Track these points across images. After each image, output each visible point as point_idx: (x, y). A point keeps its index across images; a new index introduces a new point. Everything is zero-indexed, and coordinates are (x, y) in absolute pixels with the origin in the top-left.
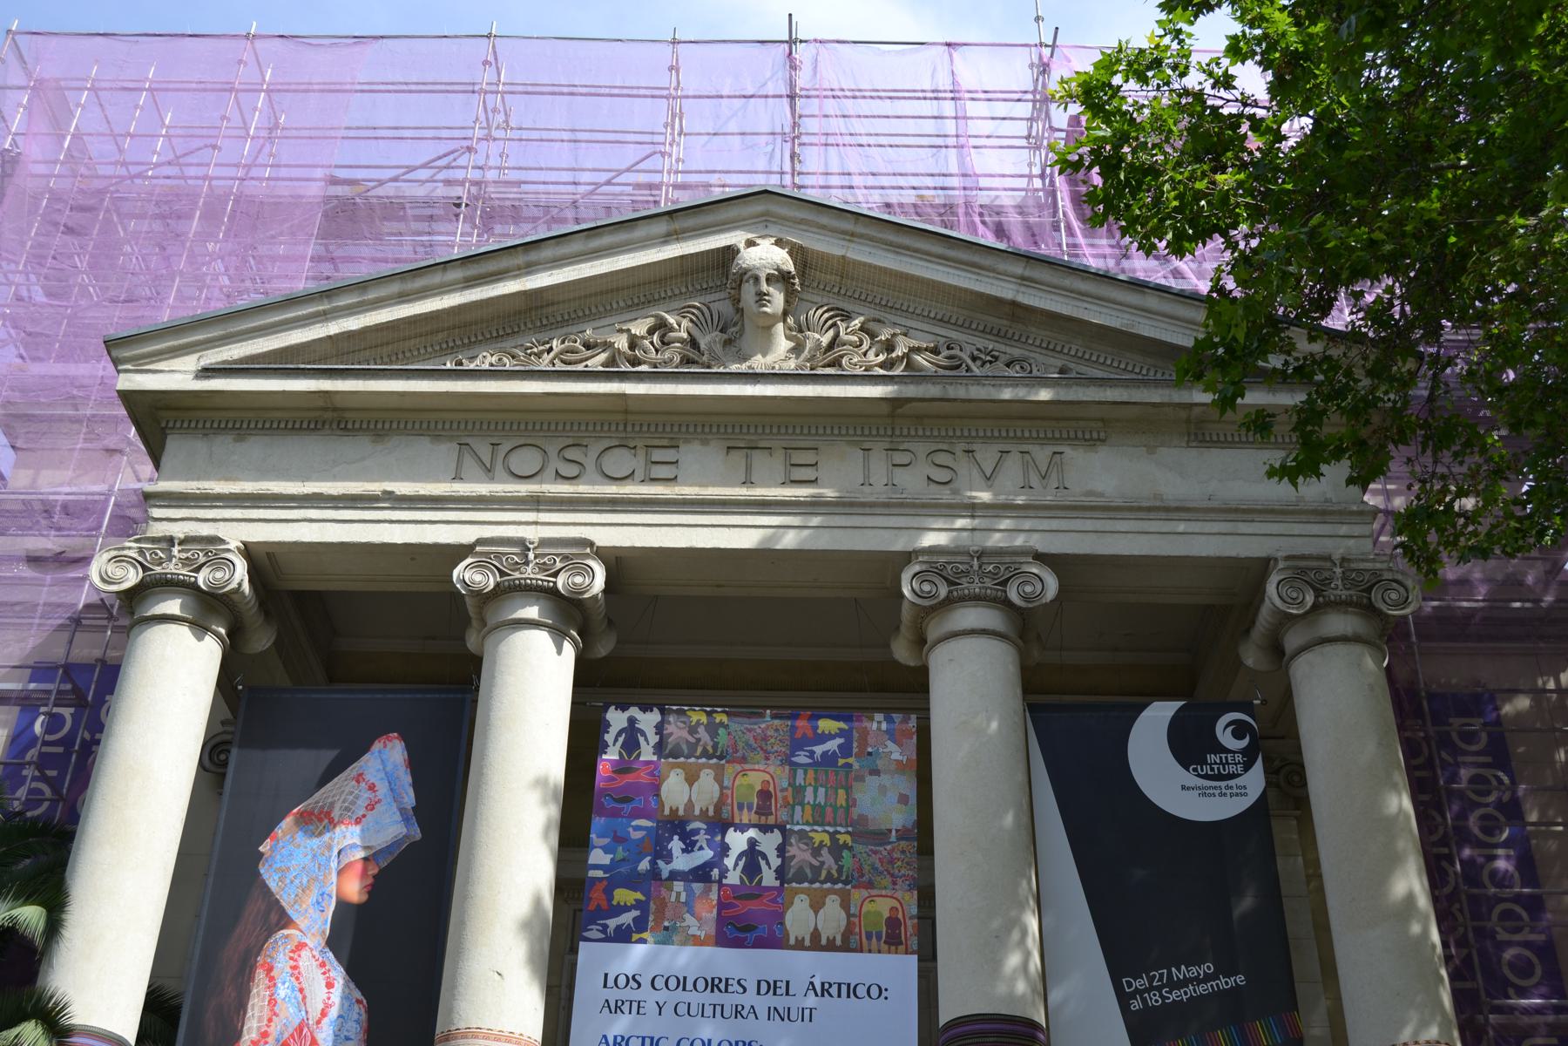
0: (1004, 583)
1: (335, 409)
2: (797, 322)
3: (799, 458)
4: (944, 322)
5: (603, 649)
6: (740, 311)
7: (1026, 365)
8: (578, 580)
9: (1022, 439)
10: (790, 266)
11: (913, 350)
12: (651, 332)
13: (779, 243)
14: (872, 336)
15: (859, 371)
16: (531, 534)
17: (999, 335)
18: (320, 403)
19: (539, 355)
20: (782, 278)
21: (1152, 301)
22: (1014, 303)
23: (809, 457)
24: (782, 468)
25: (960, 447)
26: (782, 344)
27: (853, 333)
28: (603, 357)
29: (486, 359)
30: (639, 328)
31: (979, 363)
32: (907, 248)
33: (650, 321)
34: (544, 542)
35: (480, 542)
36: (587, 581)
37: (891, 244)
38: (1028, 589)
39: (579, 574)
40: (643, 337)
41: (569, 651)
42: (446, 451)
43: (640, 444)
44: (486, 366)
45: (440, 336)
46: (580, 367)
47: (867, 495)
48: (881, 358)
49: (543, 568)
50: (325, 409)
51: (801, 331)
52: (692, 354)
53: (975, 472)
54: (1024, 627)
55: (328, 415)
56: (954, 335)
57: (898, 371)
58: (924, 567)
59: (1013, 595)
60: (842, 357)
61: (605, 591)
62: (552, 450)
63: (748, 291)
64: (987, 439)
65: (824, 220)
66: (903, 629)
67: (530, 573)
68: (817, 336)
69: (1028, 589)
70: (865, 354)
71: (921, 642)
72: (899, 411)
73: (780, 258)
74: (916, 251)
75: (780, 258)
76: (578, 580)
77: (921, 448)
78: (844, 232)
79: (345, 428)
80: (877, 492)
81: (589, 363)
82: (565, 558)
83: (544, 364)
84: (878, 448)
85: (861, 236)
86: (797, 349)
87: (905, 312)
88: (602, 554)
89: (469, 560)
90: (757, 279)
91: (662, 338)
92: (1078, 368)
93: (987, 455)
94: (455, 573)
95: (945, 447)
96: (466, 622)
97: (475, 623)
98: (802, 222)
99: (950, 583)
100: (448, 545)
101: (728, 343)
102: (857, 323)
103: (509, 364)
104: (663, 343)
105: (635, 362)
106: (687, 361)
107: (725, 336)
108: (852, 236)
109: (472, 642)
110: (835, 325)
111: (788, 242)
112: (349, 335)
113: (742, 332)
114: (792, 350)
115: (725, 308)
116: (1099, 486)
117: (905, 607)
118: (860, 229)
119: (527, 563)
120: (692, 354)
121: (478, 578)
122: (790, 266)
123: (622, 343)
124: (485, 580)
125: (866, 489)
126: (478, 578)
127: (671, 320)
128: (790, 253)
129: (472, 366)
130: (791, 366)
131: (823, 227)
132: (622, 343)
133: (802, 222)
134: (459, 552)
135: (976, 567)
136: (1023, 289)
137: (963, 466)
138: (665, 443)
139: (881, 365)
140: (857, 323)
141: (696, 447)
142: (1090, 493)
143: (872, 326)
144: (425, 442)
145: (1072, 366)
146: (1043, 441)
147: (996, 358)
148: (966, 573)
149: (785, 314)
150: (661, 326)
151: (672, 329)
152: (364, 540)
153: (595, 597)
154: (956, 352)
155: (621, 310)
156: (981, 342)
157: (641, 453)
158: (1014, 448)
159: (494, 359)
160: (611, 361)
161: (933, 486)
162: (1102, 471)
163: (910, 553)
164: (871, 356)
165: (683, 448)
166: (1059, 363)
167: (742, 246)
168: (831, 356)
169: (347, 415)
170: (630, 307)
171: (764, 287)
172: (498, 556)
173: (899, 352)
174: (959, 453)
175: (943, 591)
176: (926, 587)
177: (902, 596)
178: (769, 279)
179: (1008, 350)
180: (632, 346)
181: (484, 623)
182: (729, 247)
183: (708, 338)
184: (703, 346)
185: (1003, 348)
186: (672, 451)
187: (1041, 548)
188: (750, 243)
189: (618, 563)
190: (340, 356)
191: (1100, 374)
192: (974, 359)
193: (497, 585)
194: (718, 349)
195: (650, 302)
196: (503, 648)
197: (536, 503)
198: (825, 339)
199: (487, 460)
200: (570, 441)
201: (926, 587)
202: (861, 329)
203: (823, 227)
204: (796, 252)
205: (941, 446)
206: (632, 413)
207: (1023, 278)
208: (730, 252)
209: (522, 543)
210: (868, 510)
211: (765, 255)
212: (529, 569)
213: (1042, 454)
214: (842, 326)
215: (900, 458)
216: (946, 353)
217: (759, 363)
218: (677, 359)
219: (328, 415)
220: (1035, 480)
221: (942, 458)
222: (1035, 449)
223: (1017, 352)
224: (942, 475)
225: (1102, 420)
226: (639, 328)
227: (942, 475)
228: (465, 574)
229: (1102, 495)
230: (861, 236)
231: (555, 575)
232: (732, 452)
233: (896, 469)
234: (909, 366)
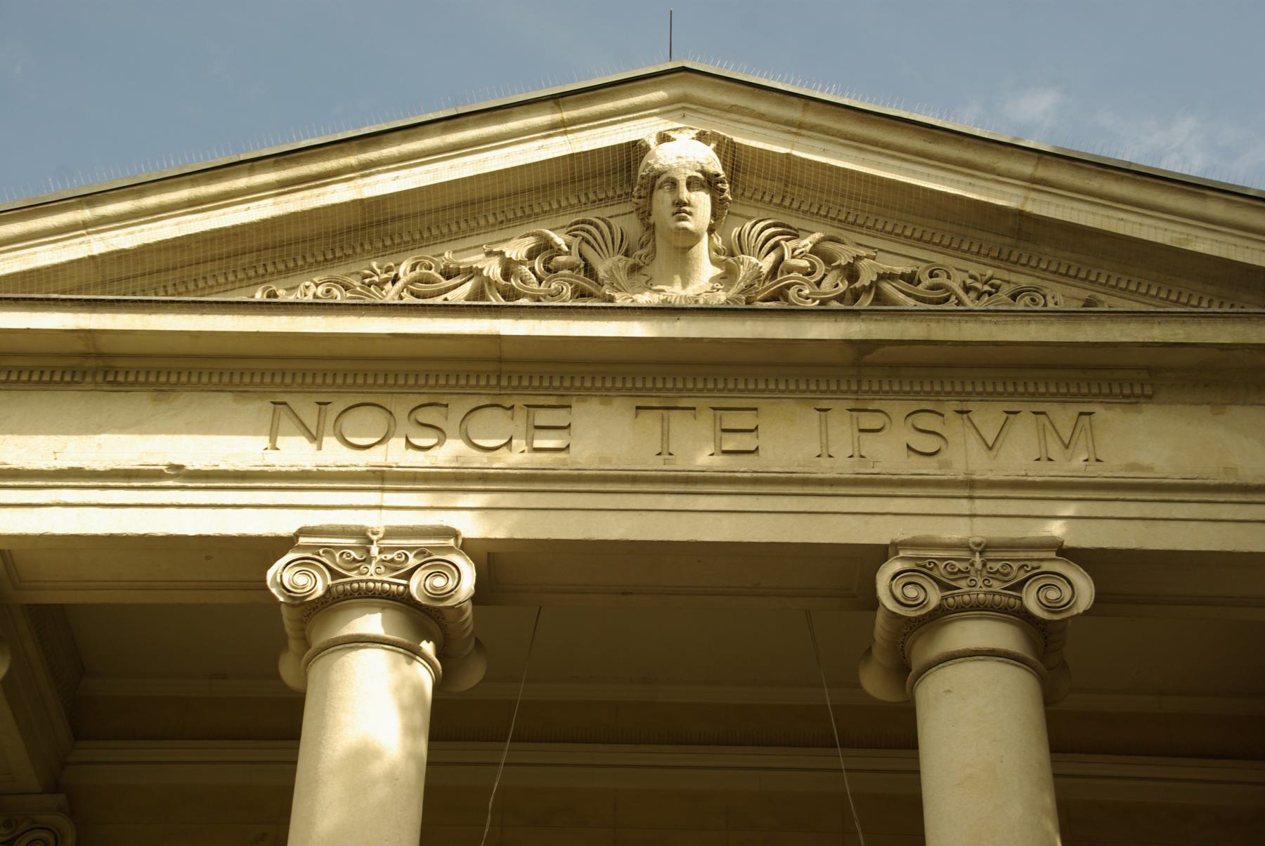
0: (1019, 586)
1: (100, 355)
2: (726, 241)
3: (732, 421)
4: (921, 242)
5: (473, 676)
6: (650, 228)
7: (1038, 297)
8: (439, 582)
9: (1034, 396)
10: (716, 166)
11: (884, 277)
12: (532, 255)
13: (702, 137)
14: (828, 259)
15: (810, 304)
16: (376, 521)
17: (1002, 259)
18: (80, 347)
19: (380, 285)
20: (708, 182)
21: (1216, 209)
22: (1020, 215)
23: (746, 420)
24: (710, 434)
25: (949, 407)
26: (705, 270)
27: (802, 255)
28: (468, 287)
29: (311, 288)
30: (517, 249)
31: (973, 295)
32: (875, 143)
33: (530, 242)
34: (391, 533)
35: (304, 532)
36: (451, 584)
37: (852, 138)
38: (1052, 595)
39: (439, 574)
40: (521, 263)
41: (423, 676)
42: (259, 409)
43: (519, 402)
44: (309, 299)
45: (247, 259)
46: (439, 300)
47: (826, 469)
48: (843, 287)
49: (391, 566)
50: (86, 355)
51: (733, 255)
52: (587, 285)
53: (972, 438)
54: (1046, 648)
55: (91, 363)
56: (938, 259)
57: (865, 302)
58: (907, 565)
59: (1031, 602)
60: (788, 287)
61: (475, 599)
62: (401, 412)
63: (663, 198)
64: (988, 397)
65: (763, 106)
66: (876, 652)
67: (374, 575)
68: (754, 260)
69: (1052, 595)
70: (819, 283)
71: (905, 672)
72: (868, 358)
73: (708, 158)
74: (886, 146)
75: (708, 158)
76: (439, 582)
77: (898, 409)
78: (788, 123)
79: (114, 382)
80: (840, 466)
81: (449, 295)
82: (421, 552)
83: (390, 294)
84: (839, 409)
85: (812, 128)
86: (728, 275)
87: (872, 230)
88: (468, 547)
89: (290, 556)
90: (674, 184)
91: (546, 262)
92: (1110, 302)
93: (988, 417)
94: (270, 574)
95: (929, 406)
96: (283, 645)
97: (293, 644)
98: (732, 109)
99: (944, 586)
100: (259, 539)
101: (634, 269)
102: (806, 243)
103: (339, 296)
104: (548, 270)
105: (510, 294)
106: (581, 293)
107: (631, 261)
108: (797, 128)
109: (287, 670)
110: (777, 245)
111: (715, 137)
112: (120, 256)
113: (652, 255)
114: (721, 278)
115: (629, 225)
116: (1145, 458)
117: (880, 617)
118: (811, 118)
119: (368, 560)
120: (587, 285)
121: (301, 580)
122: (716, 166)
123: (493, 269)
124: (315, 585)
125: (825, 461)
126: (301, 580)
127: (559, 240)
128: (717, 150)
129: (291, 299)
130: (721, 298)
131: (761, 116)
132: (493, 269)
133: (732, 109)
134: (276, 546)
135: (978, 565)
136: (1033, 195)
137: (954, 428)
138: (552, 401)
139: (840, 298)
140: (806, 243)
141: (594, 405)
142: (1133, 466)
143: (829, 246)
144: (226, 398)
145: (1102, 297)
146: (1064, 398)
147: (997, 288)
148: (964, 574)
149: (711, 230)
150: (544, 248)
151: (559, 252)
152: (141, 532)
153: (458, 609)
154: (942, 280)
155: (490, 228)
156: (975, 269)
157: (521, 415)
158: (1026, 408)
159: (320, 290)
160: (479, 293)
161: (915, 458)
162: (1150, 440)
163: (886, 547)
164: (827, 286)
165: (577, 408)
166: (1086, 295)
167: (652, 142)
168: (771, 286)
169: (119, 363)
170: (501, 224)
171: (685, 194)
172: (329, 550)
173: (866, 279)
174: (950, 414)
175: (935, 597)
176: (911, 592)
177: (875, 603)
178: (691, 184)
179: (1014, 278)
180: (506, 275)
181: (305, 642)
182: (634, 144)
183: (608, 263)
184: (602, 274)
185: (1005, 275)
186: (563, 412)
187: (1069, 543)
188: (664, 138)
189: (490, 558)
190: (104, 284)
191: (1144, 308)
192: (967, 289)
193: (329, 590)
194: (622, 276)
195: (528, 216)
196: (335, 676)
197: (381, 478)
198: (766, 264)
199: (312, 424)
200: (424, 399)
201: (911, 592)
202: (815, 250)
203: (761, 116)
204: (727, 150)
205: (924, 405)
206: (508, 361)
207: (1033, 180)
208: (636, 150)
209: (363, 535)
210: (827, 490)
211: (683, 151)
212: (372, 568)
213: (1063, 416)
214: (788, 247)
215: (869, 421)
216: (927, 282)
217: (675, 292)
218: (567, 291)
219: (91, 363)
220: (1055, 449)
221: (926, 421)
222: (1054, 410)
223: (1024, 281)
224: (928, 444)
225: (1148, 368)
226: (517, 249)
227: (928, 444)
228: (284, 575)
229: (1150, 469)
230: (812, 128)
231: (409, 575)
232: (643, 413)
233: (864, 435)
234: (880, 298)
